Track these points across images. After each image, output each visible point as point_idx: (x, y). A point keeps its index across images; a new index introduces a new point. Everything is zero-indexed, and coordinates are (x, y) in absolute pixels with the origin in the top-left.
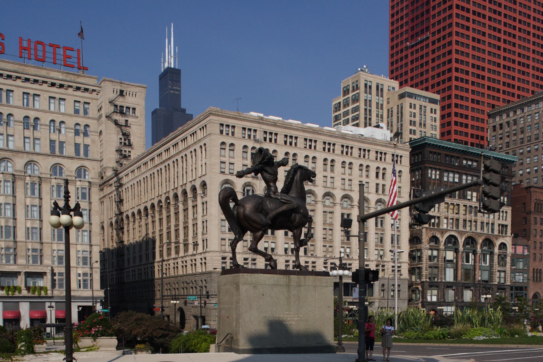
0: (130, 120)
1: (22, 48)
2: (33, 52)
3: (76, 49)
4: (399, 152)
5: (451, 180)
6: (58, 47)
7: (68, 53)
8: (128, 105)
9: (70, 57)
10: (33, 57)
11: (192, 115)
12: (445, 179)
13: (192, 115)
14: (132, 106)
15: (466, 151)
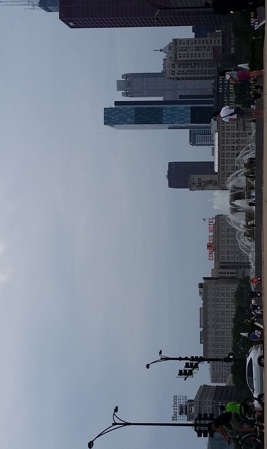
0: (203, 180)
1: (211, 232)
3: (209, 220)
6: (209, 224)
7: (210, 222)
9: (211, 221)
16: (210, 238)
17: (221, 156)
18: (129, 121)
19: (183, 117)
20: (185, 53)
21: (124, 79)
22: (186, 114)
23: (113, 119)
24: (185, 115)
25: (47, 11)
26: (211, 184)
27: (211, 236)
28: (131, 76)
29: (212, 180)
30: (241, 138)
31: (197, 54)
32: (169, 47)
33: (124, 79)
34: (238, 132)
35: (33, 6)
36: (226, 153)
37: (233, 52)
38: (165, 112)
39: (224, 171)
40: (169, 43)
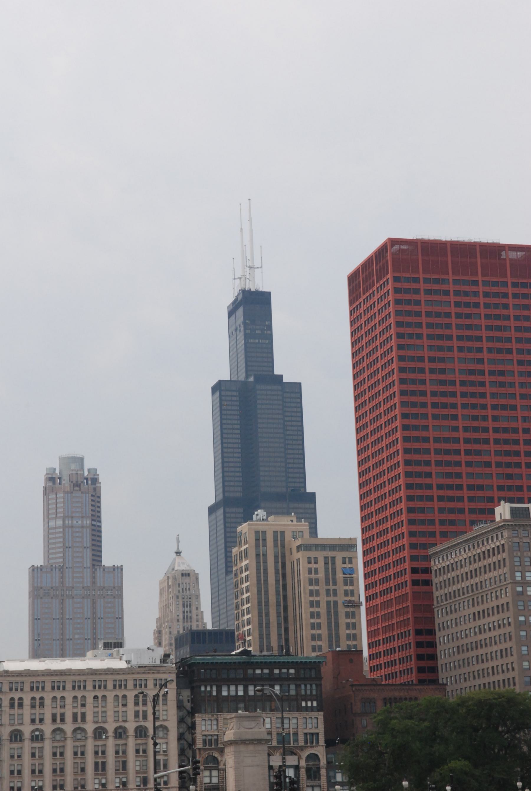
5: (233, 693)
12: (225, 693)
15: (248, 662)
17: (56, 679)
20: (321, 575)
21: (86, 473)
25: (231, 307)
28: (95, 489)
31: (317, 610)
32: (187, 573)
33: (86, 473)
34: (131, 732)
36: (65, 694)
39: (8, 690)
40: (196, 572)
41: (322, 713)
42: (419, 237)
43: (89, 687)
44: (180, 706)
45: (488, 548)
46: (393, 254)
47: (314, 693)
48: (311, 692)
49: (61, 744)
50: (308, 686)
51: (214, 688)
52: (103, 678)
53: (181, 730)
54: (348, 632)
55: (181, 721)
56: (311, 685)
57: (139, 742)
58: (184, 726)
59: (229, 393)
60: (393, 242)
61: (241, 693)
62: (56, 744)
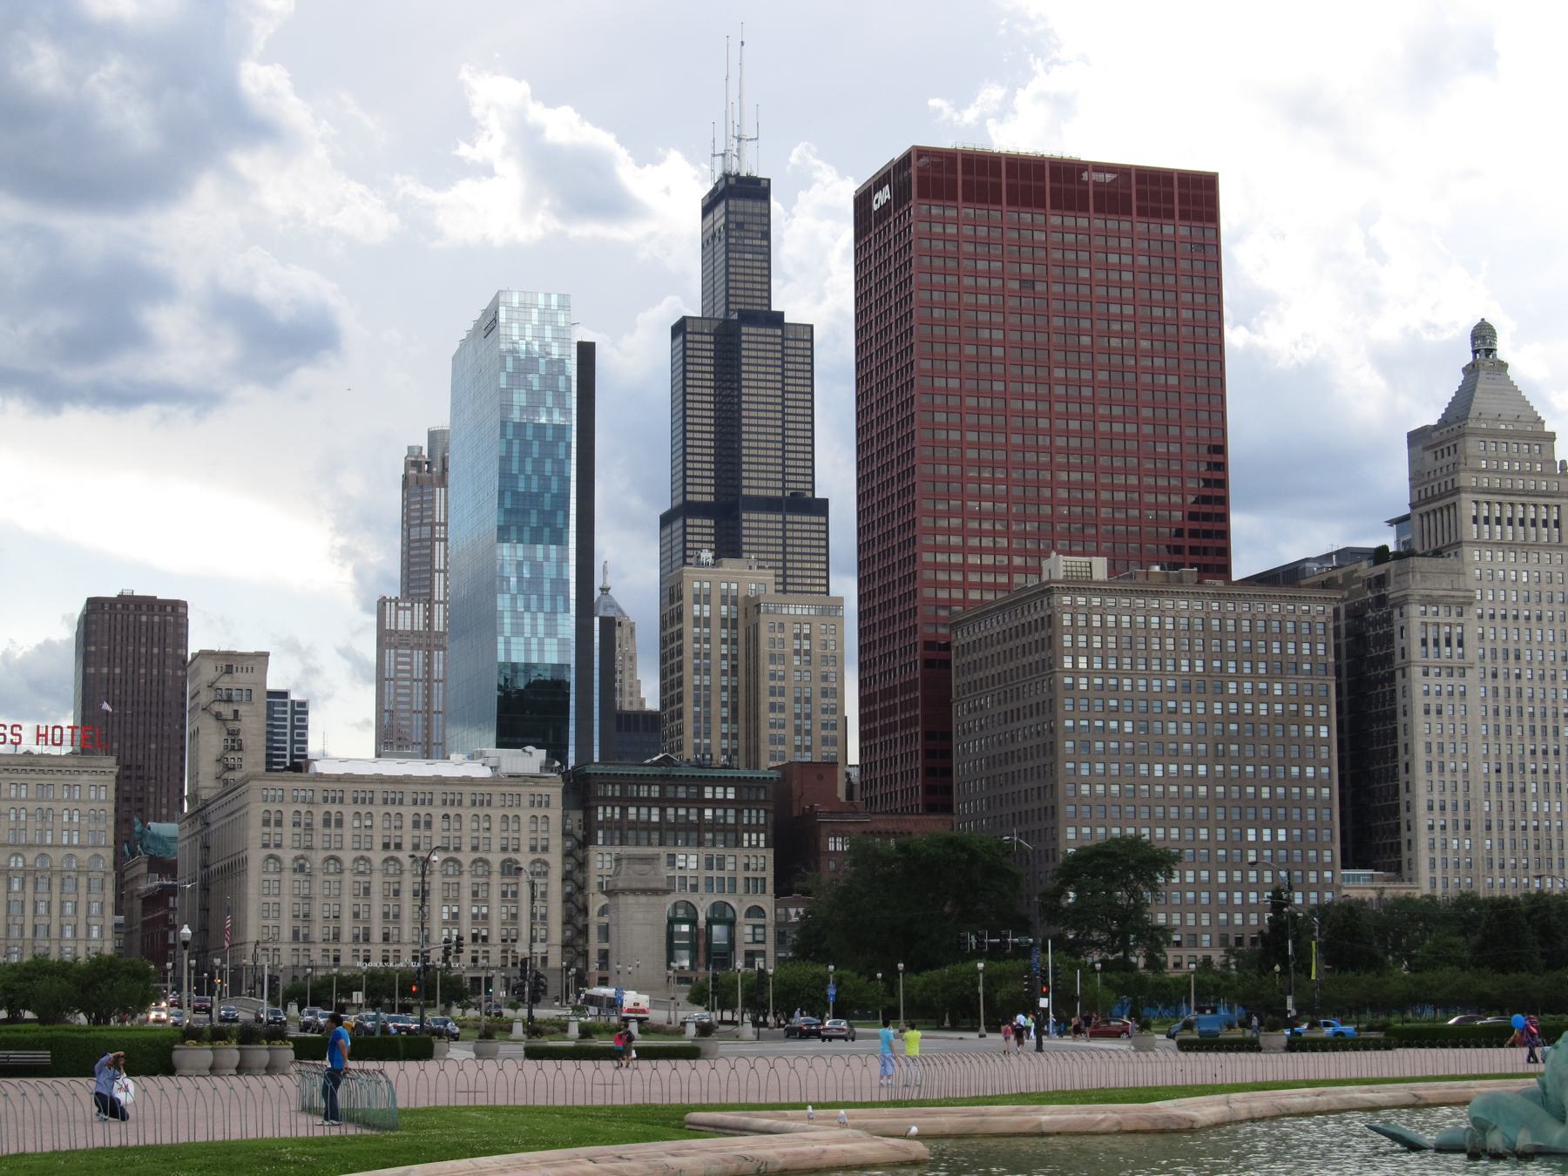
0: (242, 709)
1: (39, 735)
2: (50, 737)
4: (544, 791)
8: (239, 686)
10: (50, 742)
11: (811, 327)
13: (811, 327)
14: (244, 687)
16: (9, 729)
18: (516, 397)
19: (527, 630)
22: (541, 643)
23: (522, 328)
24: (534, 641)
25: (707, 201)
26: (226, 747)
27: (19, 735)
29: (240, 749)
30: (466, 880)
34: (496, 866)
35: (723, 155)
36: (402, 809)
37: (831, 847)
38: (547, 558)
41: (771, 851)
42: (960, 147)
43: (437, 801)
44: (566, 834)
45: (1029, 619)
46: (919, 170)
47: (762, 821)
48: (758, 819)
49: (396, 879)
50: (754, 813)
51: (617, 810)
52: (456, 789)
53: (568, 867)
54: (824, 733)
55: (567, 854)
56: (758, 812)
57: (507, 881)
58: (572, 860)
59: (698, 338)
60: (921, 152)
61: (655, 818)
62: (387, 879)
